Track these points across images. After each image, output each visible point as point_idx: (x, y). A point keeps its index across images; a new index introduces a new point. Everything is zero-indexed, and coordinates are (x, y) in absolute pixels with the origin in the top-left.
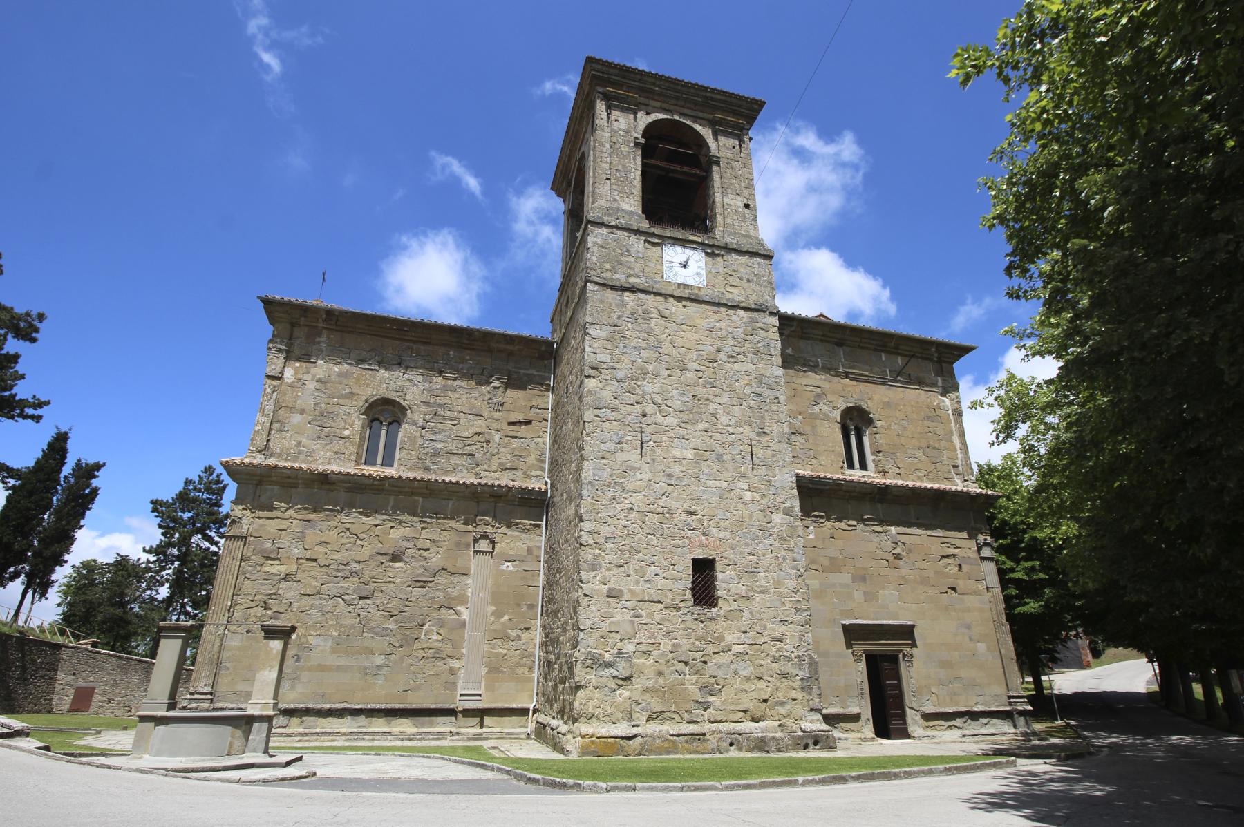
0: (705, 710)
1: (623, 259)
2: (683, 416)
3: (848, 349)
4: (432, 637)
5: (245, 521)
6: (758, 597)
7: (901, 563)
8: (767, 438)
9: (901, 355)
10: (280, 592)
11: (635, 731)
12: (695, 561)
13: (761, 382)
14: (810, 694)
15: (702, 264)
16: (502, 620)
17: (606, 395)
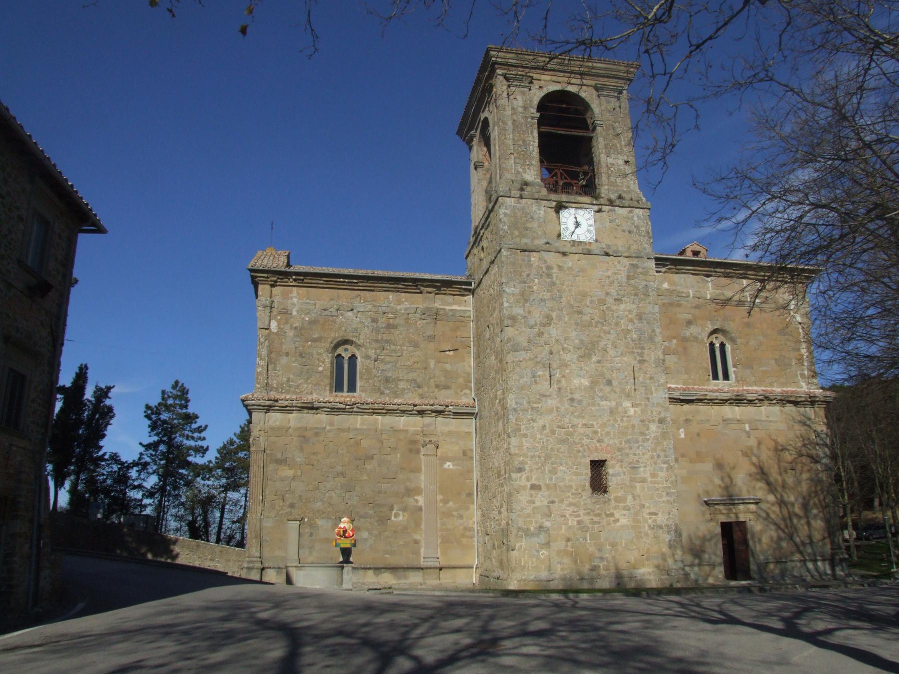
1: (529, 225)
2: (580, 353)
4: (400, 518)
6: (638, 485)
12: (592, 462)
13: (641, 319)
15: (592, 222)
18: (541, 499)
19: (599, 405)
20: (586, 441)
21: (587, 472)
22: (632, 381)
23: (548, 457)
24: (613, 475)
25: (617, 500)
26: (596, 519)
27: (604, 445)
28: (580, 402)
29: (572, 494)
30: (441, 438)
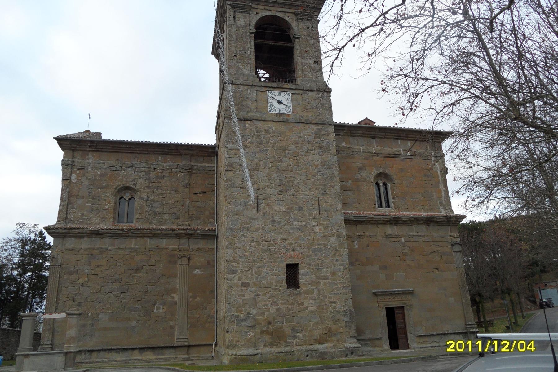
0: (294, 340)
1: (244, 103)
2: (280, 188)
3: (378, 140)
4: (160, 310)
5: (59, 257)
6: (322, 282)
9: (410, 140)
10: (80, 292)
12: (287, 265)
13: (324, 165)
14: (350, 329)
16: (196, 300)
18: (249, 294)
19: (292, 224)
20: (283, 250)
22: (318, 208)
23: (255, 262)
24: (302, 275)
25: (306, 292)
26: (290, 307)
27: (296, 253)
28: (279, 223)
29: (273, 289)
30: (192, 253)
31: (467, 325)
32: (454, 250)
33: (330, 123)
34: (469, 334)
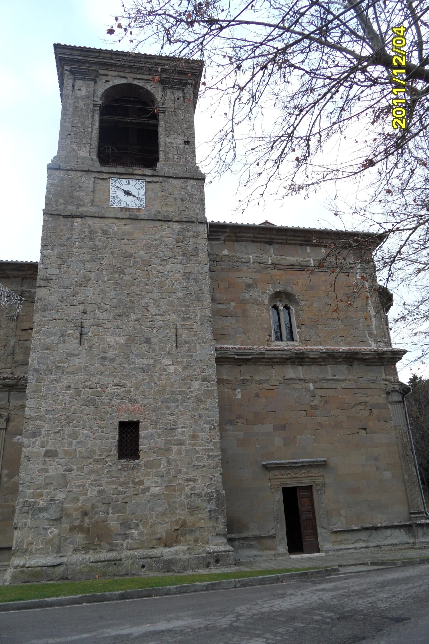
0: (125, 540)
1: (75, 194)
2: (118, 311)
3: (277, 246)
6: (175, 449)
7: (318, 412)
8: (191, 322)
11: (59, 561)
12: (122, 424)
17: (54, 300)
18: (55, 469)
19: (134, 362)
20: (116, 401)
21: (114, 435)
22: (174, 338)
23: (69, 419)
24: (144, 438)
25: (148, 465)
26: (120, 488)
27: (136, 405)
28: (112, 360)
29: (95, 460)
31: (411, 513)
32: (391, 400)
33: (199, 221)
34: (415, 528)
